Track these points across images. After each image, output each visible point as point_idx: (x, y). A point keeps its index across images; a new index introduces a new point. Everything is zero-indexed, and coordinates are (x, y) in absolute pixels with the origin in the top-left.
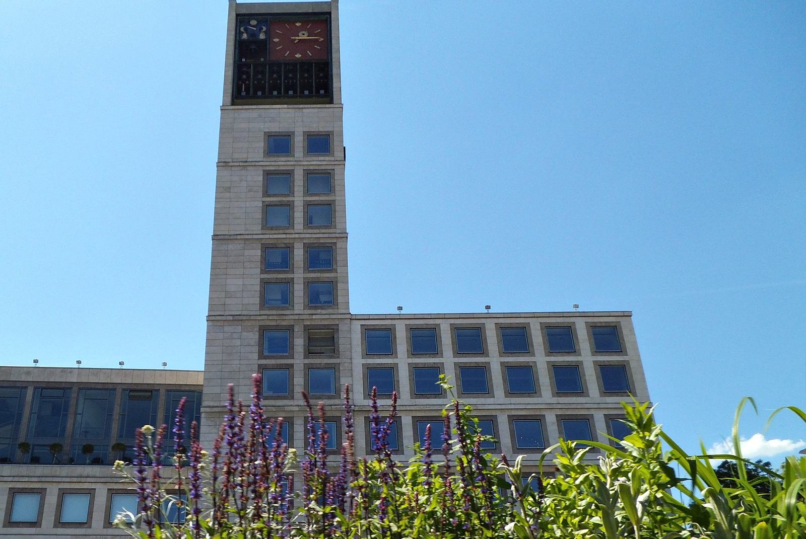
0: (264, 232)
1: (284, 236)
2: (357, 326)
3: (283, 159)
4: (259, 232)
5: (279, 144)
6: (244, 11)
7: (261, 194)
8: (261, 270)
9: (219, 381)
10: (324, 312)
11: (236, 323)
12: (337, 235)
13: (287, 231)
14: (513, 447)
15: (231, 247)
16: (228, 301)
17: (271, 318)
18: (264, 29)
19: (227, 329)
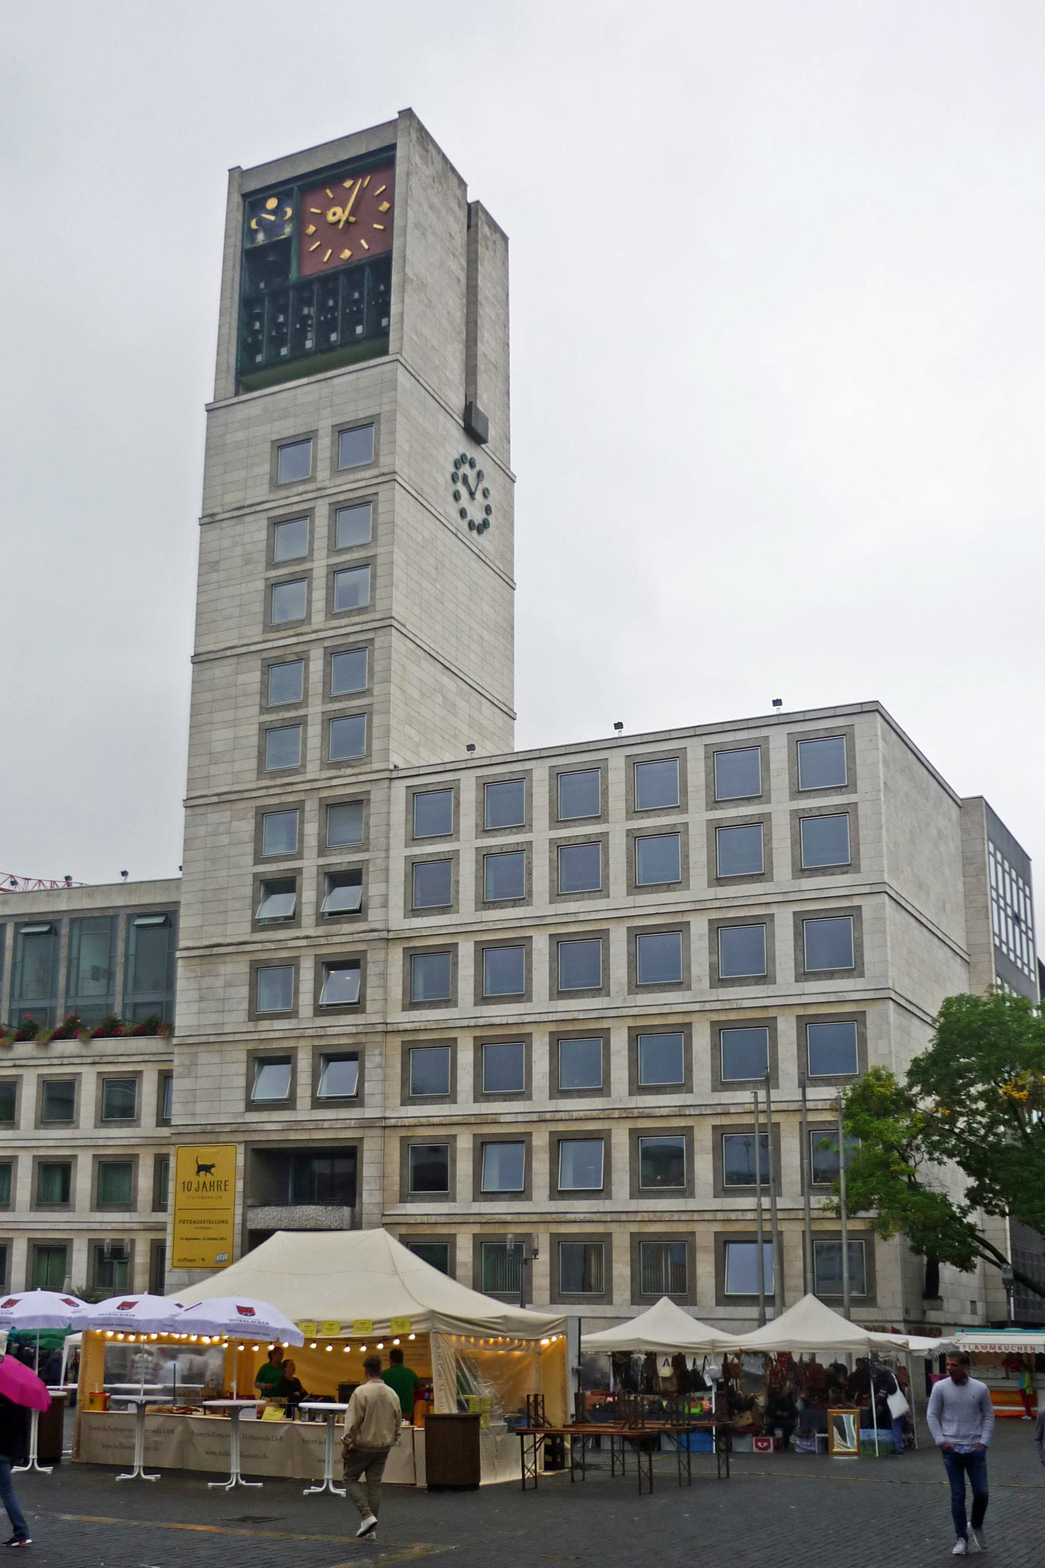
2: (399, 791)
6: (253, 185)
7: (264, 564)
8: (261, 707)
9: (201, 906)
11: (224, 806)
12: (377, 624)
13: (300, 630)
14: (629, 982)
17: (272, 791)
18: (289, 212)
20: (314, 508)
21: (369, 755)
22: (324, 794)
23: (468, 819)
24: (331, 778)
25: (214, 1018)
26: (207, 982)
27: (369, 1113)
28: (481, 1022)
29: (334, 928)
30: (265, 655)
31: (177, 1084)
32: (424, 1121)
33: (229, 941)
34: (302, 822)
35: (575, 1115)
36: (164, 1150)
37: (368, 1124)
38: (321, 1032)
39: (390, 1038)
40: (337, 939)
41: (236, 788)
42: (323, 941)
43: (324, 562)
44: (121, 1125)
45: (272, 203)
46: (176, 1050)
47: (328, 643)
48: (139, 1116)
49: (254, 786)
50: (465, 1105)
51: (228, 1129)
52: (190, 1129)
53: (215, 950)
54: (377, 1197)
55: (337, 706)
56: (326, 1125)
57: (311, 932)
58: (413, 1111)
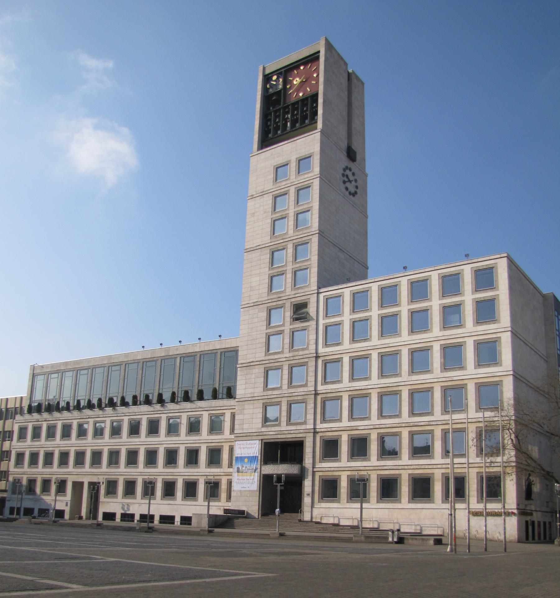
0: (274, 240)
1: (282, 241)
4: (269, 241)
10: (302, 291)
20: (289, 190)
21: (310, 284)
22: (293, 300)
23: (347, 307)
24: (295, 294)
28: (352, 389)
29: (296, 353)
30: (271, 247)
31: (237, 417)
32: (329, 429)
33: (257, 360)
34: (284, 312)
35: (388, 426)
36: (232, 444)
37: (307, 431)
38: (291, 395)
40: (297, 358)
41: (260, 300)
42: (292, 358)
43: (293, 210)
44: (217, 434)
45: (275, 78)
46: (237, 403)
47: (294, 241)
48: (224, 430)
49: (266, 298)
50: (345, 423)
52: (242, 435)
53: (252, 364)
55: (297, 265)
56: (292, 432)
57: (287, 355)
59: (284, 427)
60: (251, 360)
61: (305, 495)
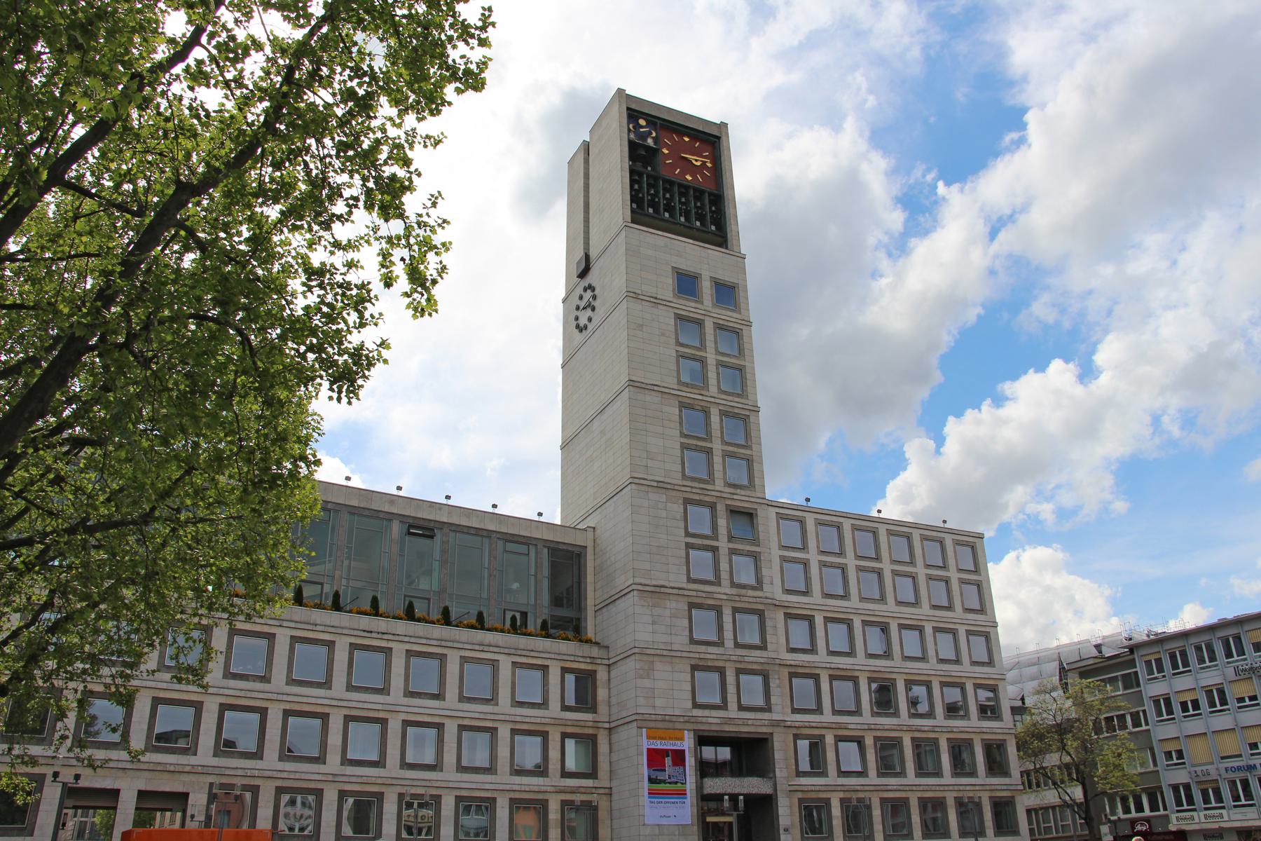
3: (693, 304)
5: (687, 283)
10: (743, 492)
15: (648, 398)
16: (650, 463)
19: (653, 496)
22: (729, 502)
25: (665, 638)
26: (657, 611)
27: (775, 716)
39: (782, 669)
51: (681, 719)
53: (663, 590)
54: (785, 774)
57: (728, 591)
58: (799, 717)
59: (733, 712)
60: (661, 583)
61: (781, 831)
